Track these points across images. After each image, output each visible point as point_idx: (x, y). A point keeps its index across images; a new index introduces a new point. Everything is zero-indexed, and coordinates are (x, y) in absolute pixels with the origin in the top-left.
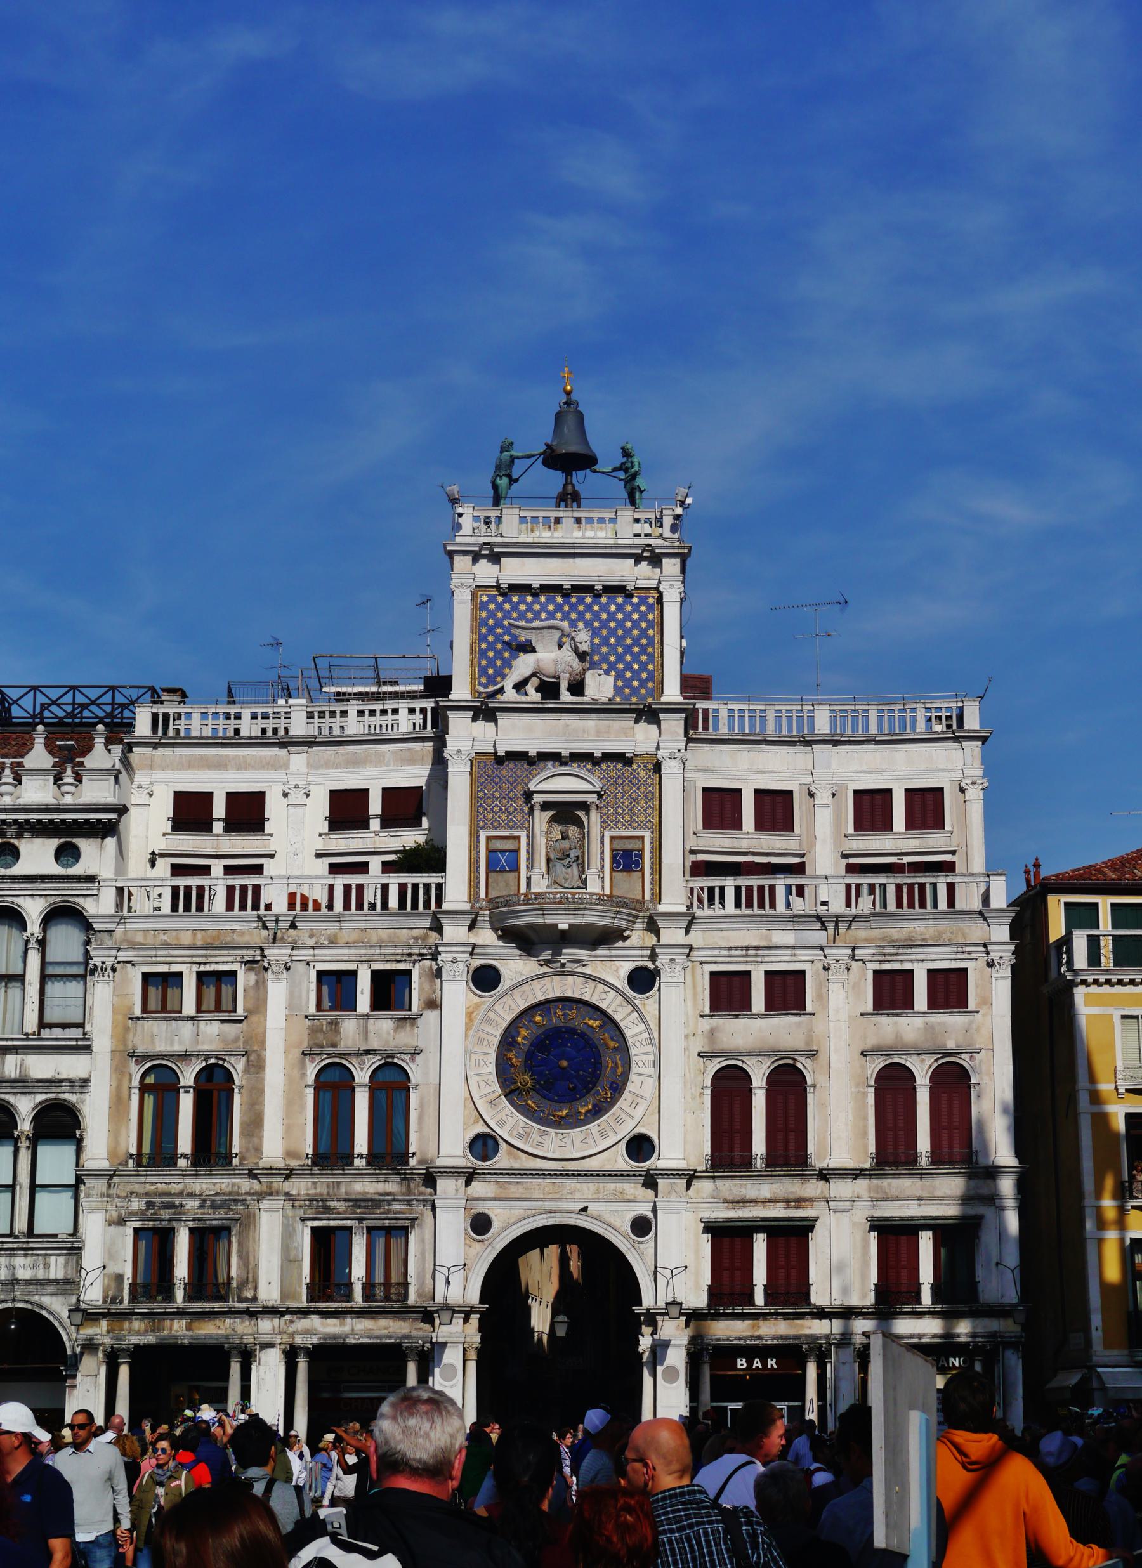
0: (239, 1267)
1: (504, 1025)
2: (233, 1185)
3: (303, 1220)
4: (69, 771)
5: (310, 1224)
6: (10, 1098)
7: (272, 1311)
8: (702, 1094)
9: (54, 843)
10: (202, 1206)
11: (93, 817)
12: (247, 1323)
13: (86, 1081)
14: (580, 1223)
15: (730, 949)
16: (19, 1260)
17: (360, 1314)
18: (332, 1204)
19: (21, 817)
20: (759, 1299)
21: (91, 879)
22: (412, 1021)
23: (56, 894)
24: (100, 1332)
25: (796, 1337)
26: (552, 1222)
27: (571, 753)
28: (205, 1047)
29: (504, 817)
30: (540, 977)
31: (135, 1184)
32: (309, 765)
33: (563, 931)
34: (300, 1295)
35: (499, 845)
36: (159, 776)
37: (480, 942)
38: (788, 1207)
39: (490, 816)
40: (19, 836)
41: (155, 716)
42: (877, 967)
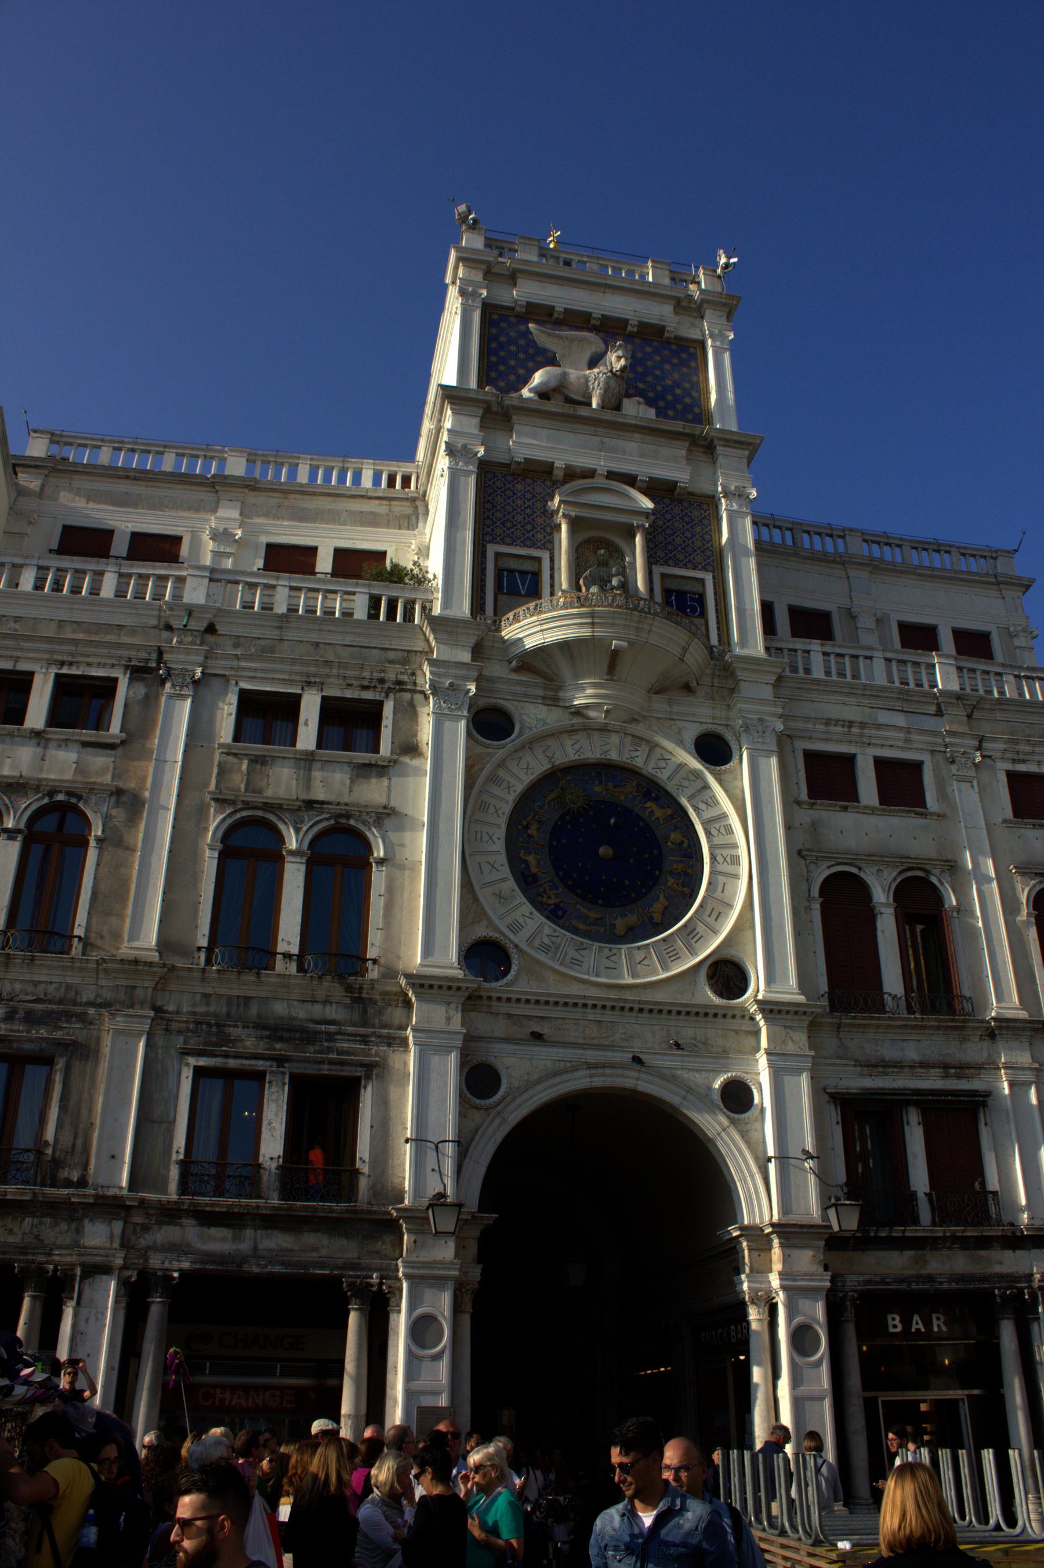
0: (59, 1126)
1: (520, 788)
2: (68, 987)
3: (185, 1053)
5: (192, 1061)
7: (110, 1207)
8: (808, 909)
12: (64, 1226)
14: (643, 1086)
15: (828, 722)
17: (270, 1221)
18: (235, 1032)
20: (925, 1214)
22: (381, 769)
25: (985, 1279)
26: (598, 1082)
27: (609, 472)
29: (518, 533)
30: (572, 731)
32: (241, 514)
33: (615, 654)
34: (165, 1181)
35: (513, 564)
37: (485, 673)
38: (946, 1076)
39: (498, 531)
42: (1010, 767)
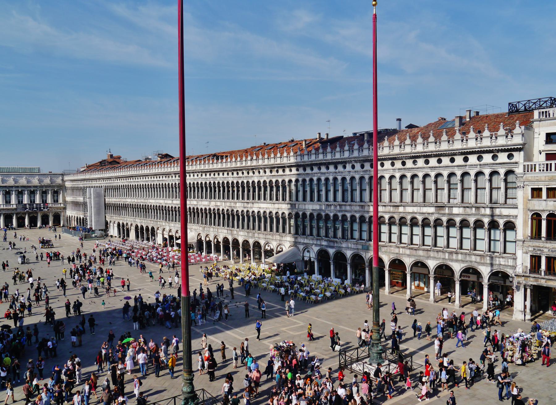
4: (510, 135)
6: (498, 220)
9: (507, 154)
10: (549, 251)
11: (516, 147)
13: (517, 216)
16: (501, 259)
19: (497, 148)
21: (516, 163)
23: (508, 167)
24: (522, 280)
28: (549, 208)
31: (530, 244)
36: (541, 129)
40: (498, 152)
41: (540, 113)
